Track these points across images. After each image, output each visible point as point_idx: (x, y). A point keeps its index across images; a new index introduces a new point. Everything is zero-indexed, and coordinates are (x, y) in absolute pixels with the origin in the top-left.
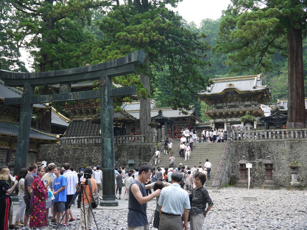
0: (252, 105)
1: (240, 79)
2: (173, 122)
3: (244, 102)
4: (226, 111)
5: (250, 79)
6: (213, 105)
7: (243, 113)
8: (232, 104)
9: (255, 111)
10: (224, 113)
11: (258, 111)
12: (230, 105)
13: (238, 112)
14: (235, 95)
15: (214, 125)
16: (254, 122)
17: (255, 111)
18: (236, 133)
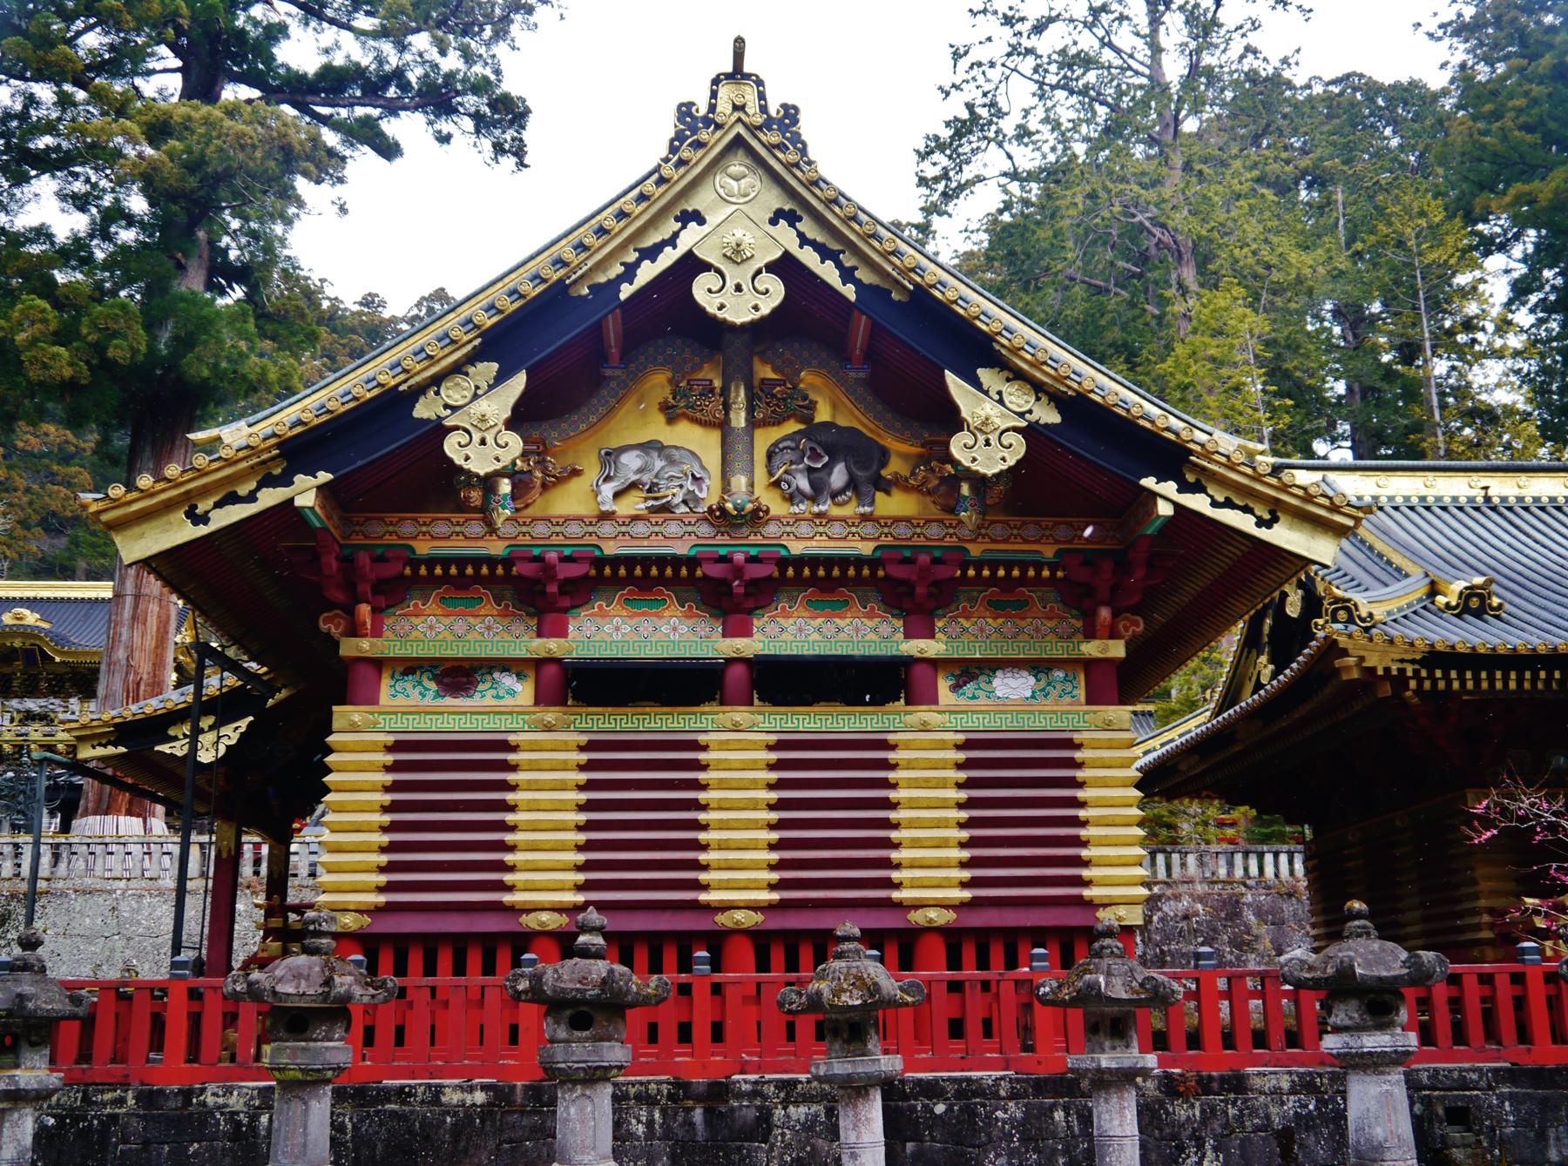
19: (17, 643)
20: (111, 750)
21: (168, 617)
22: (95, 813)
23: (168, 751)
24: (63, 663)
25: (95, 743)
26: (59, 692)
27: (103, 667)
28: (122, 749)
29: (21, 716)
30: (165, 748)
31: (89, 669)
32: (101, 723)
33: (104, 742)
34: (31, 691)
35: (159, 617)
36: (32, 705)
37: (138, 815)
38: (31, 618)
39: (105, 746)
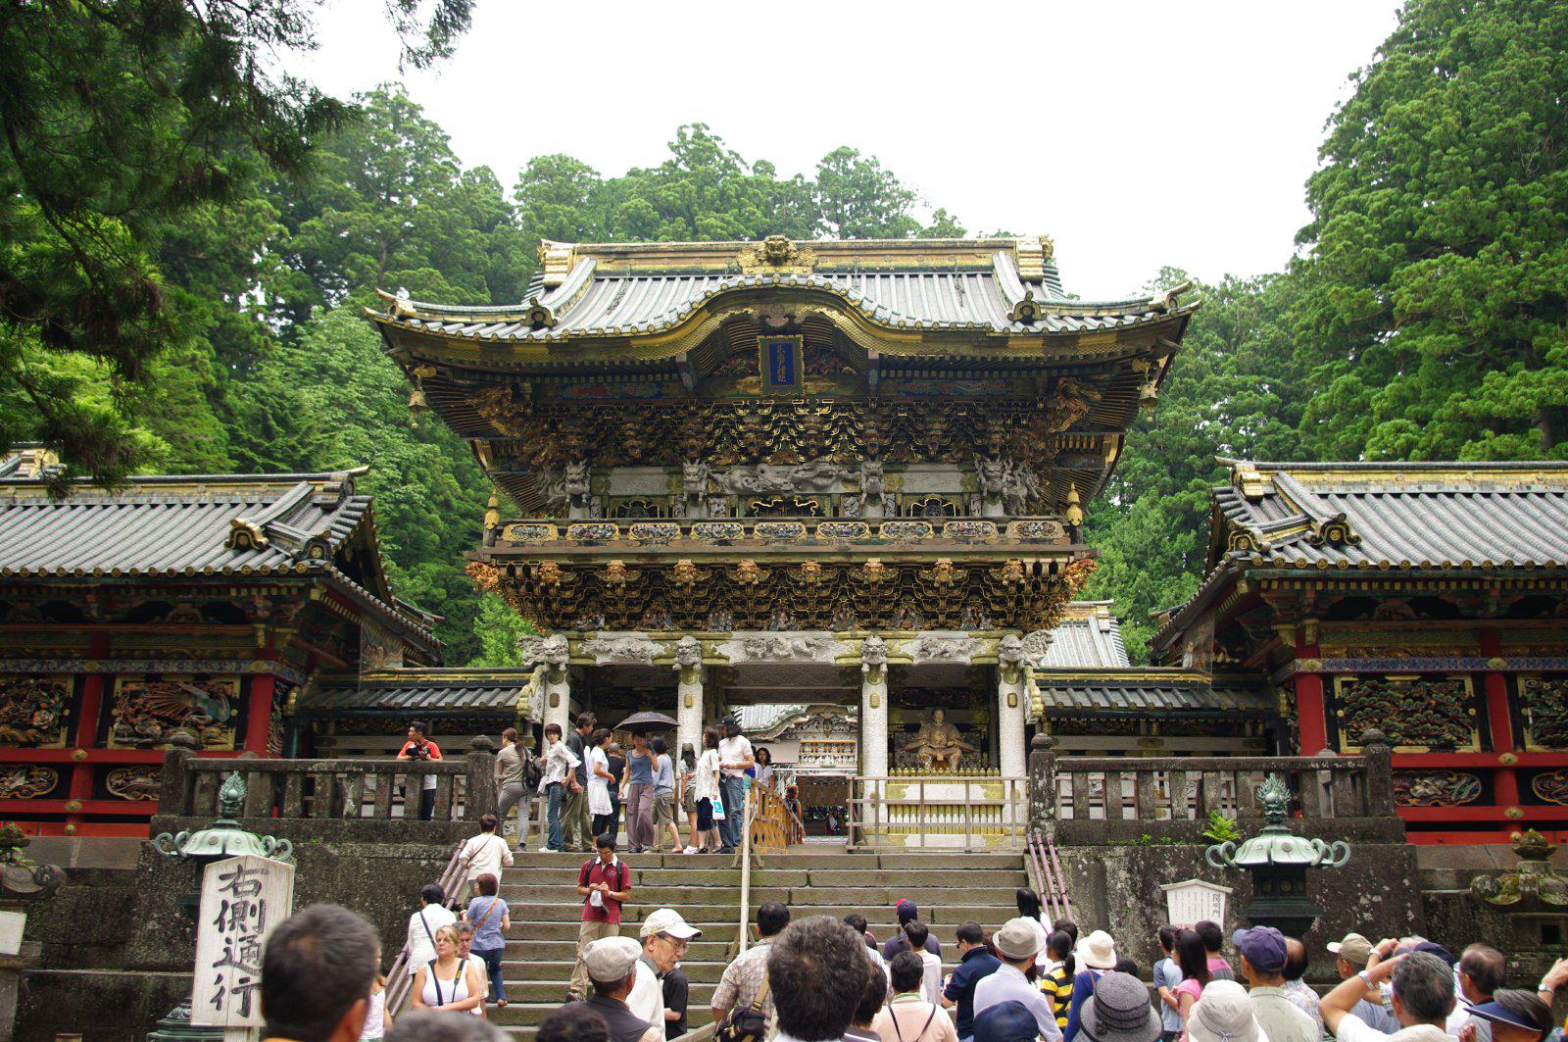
0: (975, 507)
1: (847, 262)
3: (894, 466)
4: (708, 546)
5: (943, 271)
6: (574, 471)
7: (892, 574)
8: (772, 475)
9: (1030, 561)
10: (684, 563)
11: (1053, 567)
12: (745, 495)
13: (843, 570)
14: (811, 388)
15: (563, 690)
16: (1005, 689)
17: (1030, 561)
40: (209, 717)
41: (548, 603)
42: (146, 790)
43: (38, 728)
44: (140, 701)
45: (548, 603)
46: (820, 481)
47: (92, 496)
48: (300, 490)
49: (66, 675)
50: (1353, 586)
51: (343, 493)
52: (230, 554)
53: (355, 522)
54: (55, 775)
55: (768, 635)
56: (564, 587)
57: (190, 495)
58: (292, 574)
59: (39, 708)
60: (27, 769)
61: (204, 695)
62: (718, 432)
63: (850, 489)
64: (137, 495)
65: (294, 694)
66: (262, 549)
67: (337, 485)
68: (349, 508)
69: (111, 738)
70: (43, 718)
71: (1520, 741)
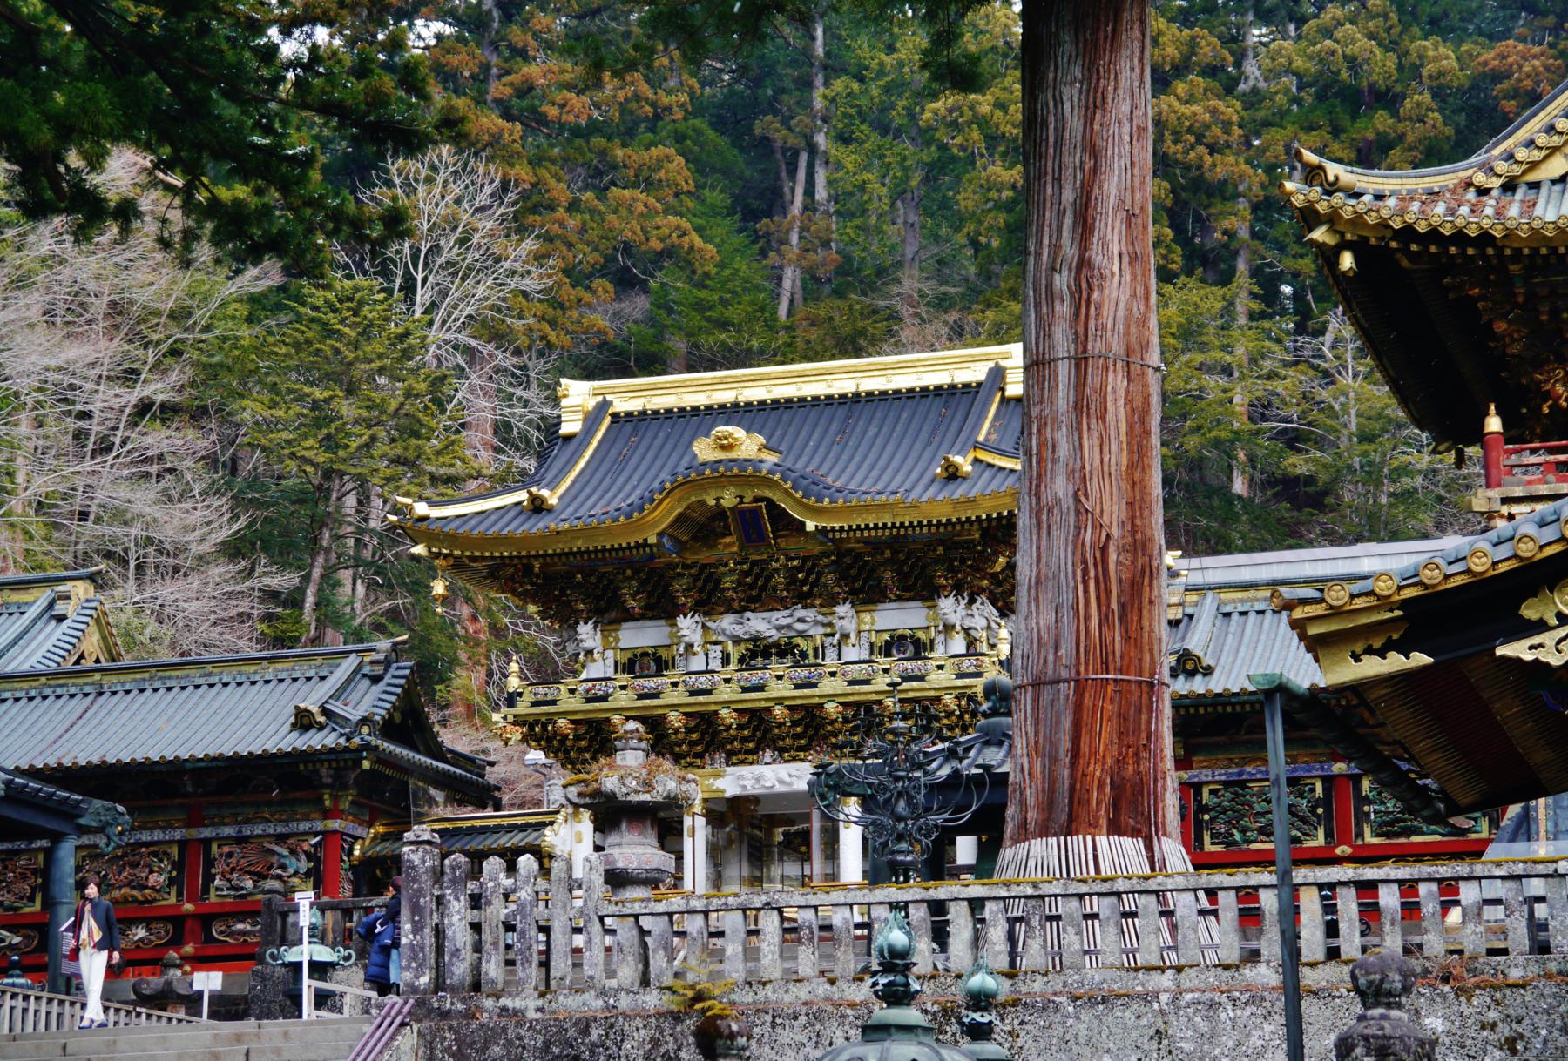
2: (69, 814)
18: (476, 927)
19: (729, 500)
20: (1395, 662)
21: (1146, 399)
22: (1044, 832)
23: (1528, 657)
24: (822, 532)
25: (1359, 648)
26: (809, 594)
27: (1023, 521)
28: (1421, 659)
29: (742, 649)
30: (1518, 650)
31: (867, 542)
32: (1372, 601)
33: (1377, 645)
34: (757, 597)
35: (1129, 401)
36: (761, 624)
37: (1134, 833)
38: (748, 444)
39: (1382, 653)
40: (291, 871)
41: (567, 752)
42: (244, 933)
43: (153, 888)
44: (233, 860)
45: (567, 752)
46: (800, 626)
47: (170, 678)
48: (350, 663)
49: (170, 842)
50: (1220, 709)
51: (387, 663)
52: (295, 734)
53: (399, 690)
54: (170, 927)
55: (757, 769)
56: (577, 737)
57: (255, 672)
58: (346, 749)
59: (151, 872)
60: (148, 922)
61: (286, 853)
62: (710, 586)
63: (829, 630)
64: (210, 674)
65: (357, 847)
66: (321, 727)
67: (381, 656)
68: (394, 677)
69: (213, 893)
70: (157, 879)
71: (1360, 834)
